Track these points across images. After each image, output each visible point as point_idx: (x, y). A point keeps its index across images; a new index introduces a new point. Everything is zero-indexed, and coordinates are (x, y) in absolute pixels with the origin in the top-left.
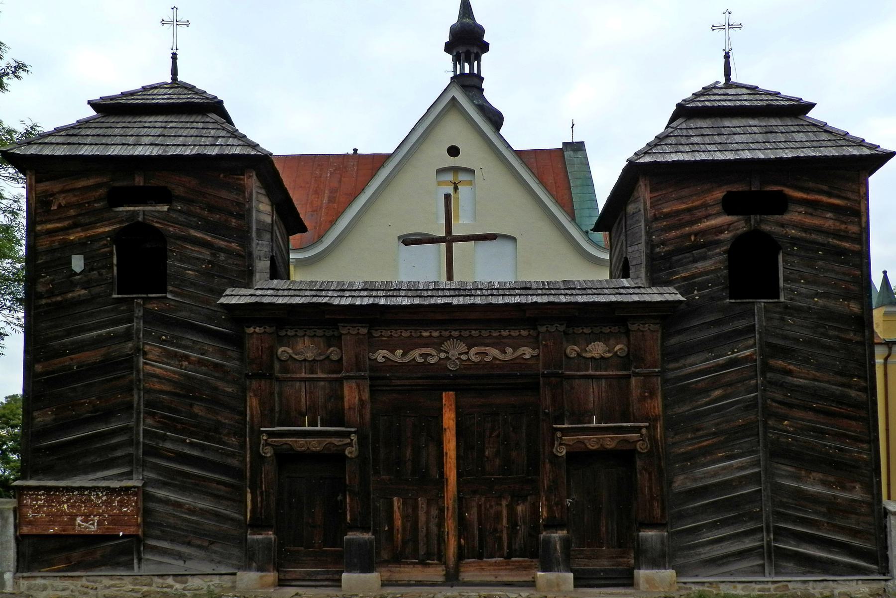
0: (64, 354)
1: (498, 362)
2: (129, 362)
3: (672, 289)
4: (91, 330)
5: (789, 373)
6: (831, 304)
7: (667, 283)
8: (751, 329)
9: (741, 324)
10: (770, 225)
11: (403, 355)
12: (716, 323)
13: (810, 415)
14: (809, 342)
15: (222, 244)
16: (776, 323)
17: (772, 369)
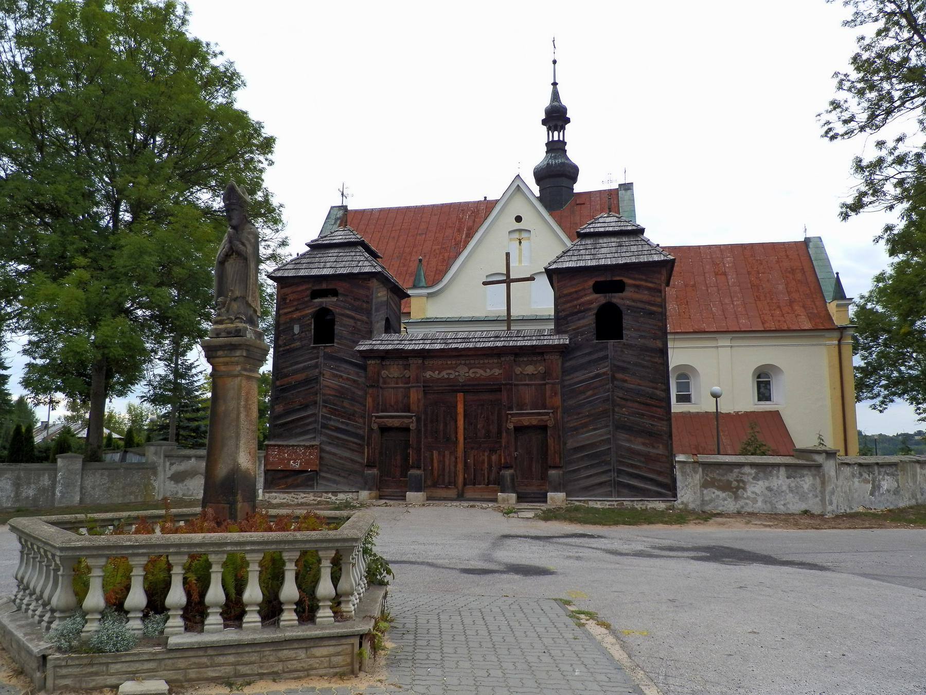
2: (316, 379)
8: (606, 357)
12: (590, 353)
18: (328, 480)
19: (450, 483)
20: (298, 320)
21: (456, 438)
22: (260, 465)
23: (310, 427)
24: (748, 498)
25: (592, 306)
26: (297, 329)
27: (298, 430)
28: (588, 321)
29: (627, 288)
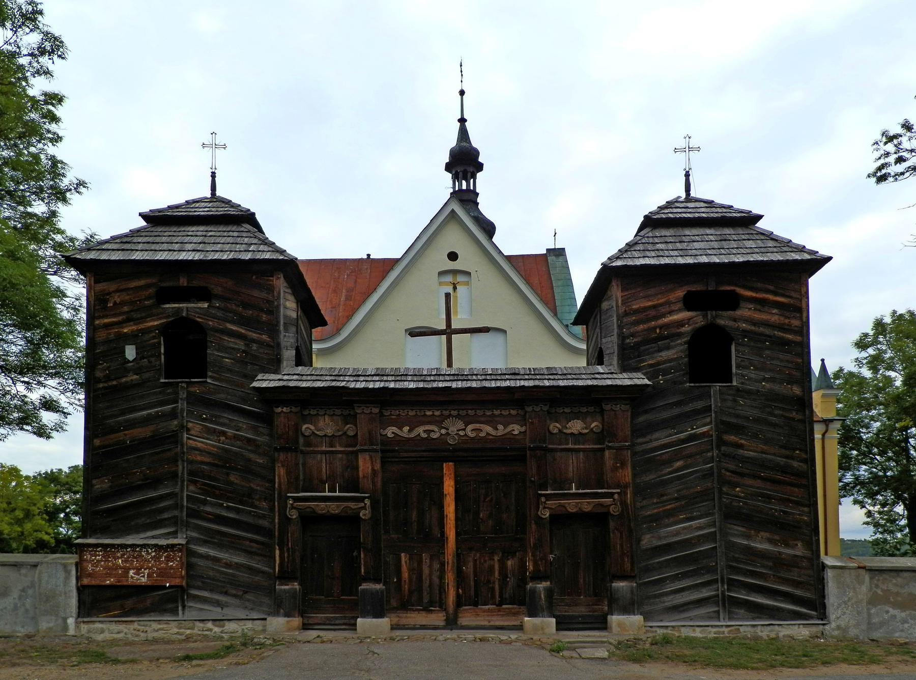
0: (119, 431)
3: (640, 375)
5: (741, 446)
6: (777, 387)
7: (636, 369)
8: (708, 409)
9: (699, 405)
10: (724, 320)
11: (410, 431)
12: (678, 404)
13: (758, 483)
14: (757, 420)
15: (255, 336)
16: (729, 404)
17: (725, 443)
25: (683, 330)
28: (675, 352)
29: (742, 304)
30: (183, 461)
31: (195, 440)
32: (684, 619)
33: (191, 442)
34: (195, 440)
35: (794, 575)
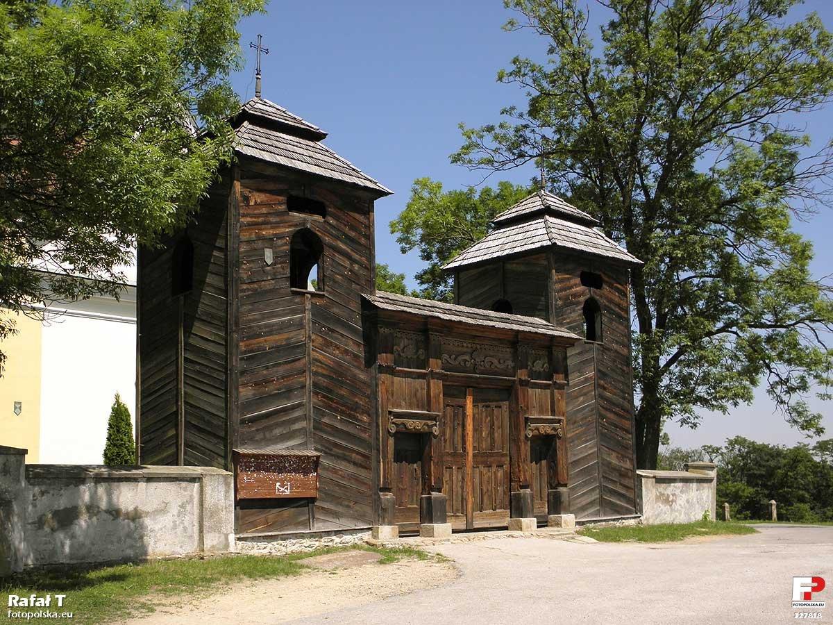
0: (260, 336)
1: (496, 369)
4: (278, 316)
5: (605, 389)
7: (561, 324)
18: (327, 512)
19: (457, 510)
20: (270, 241)
21: (464, 449)
22: (227, 492)
23: (297, 426)
24: (677, 511)
26: (269, 256)
27: (277, 431)
30: (310, 372)
31: (317, 352)
32: (588, 516)
33: (315, 353)
34: (317, 352)
35: (626, 482)
